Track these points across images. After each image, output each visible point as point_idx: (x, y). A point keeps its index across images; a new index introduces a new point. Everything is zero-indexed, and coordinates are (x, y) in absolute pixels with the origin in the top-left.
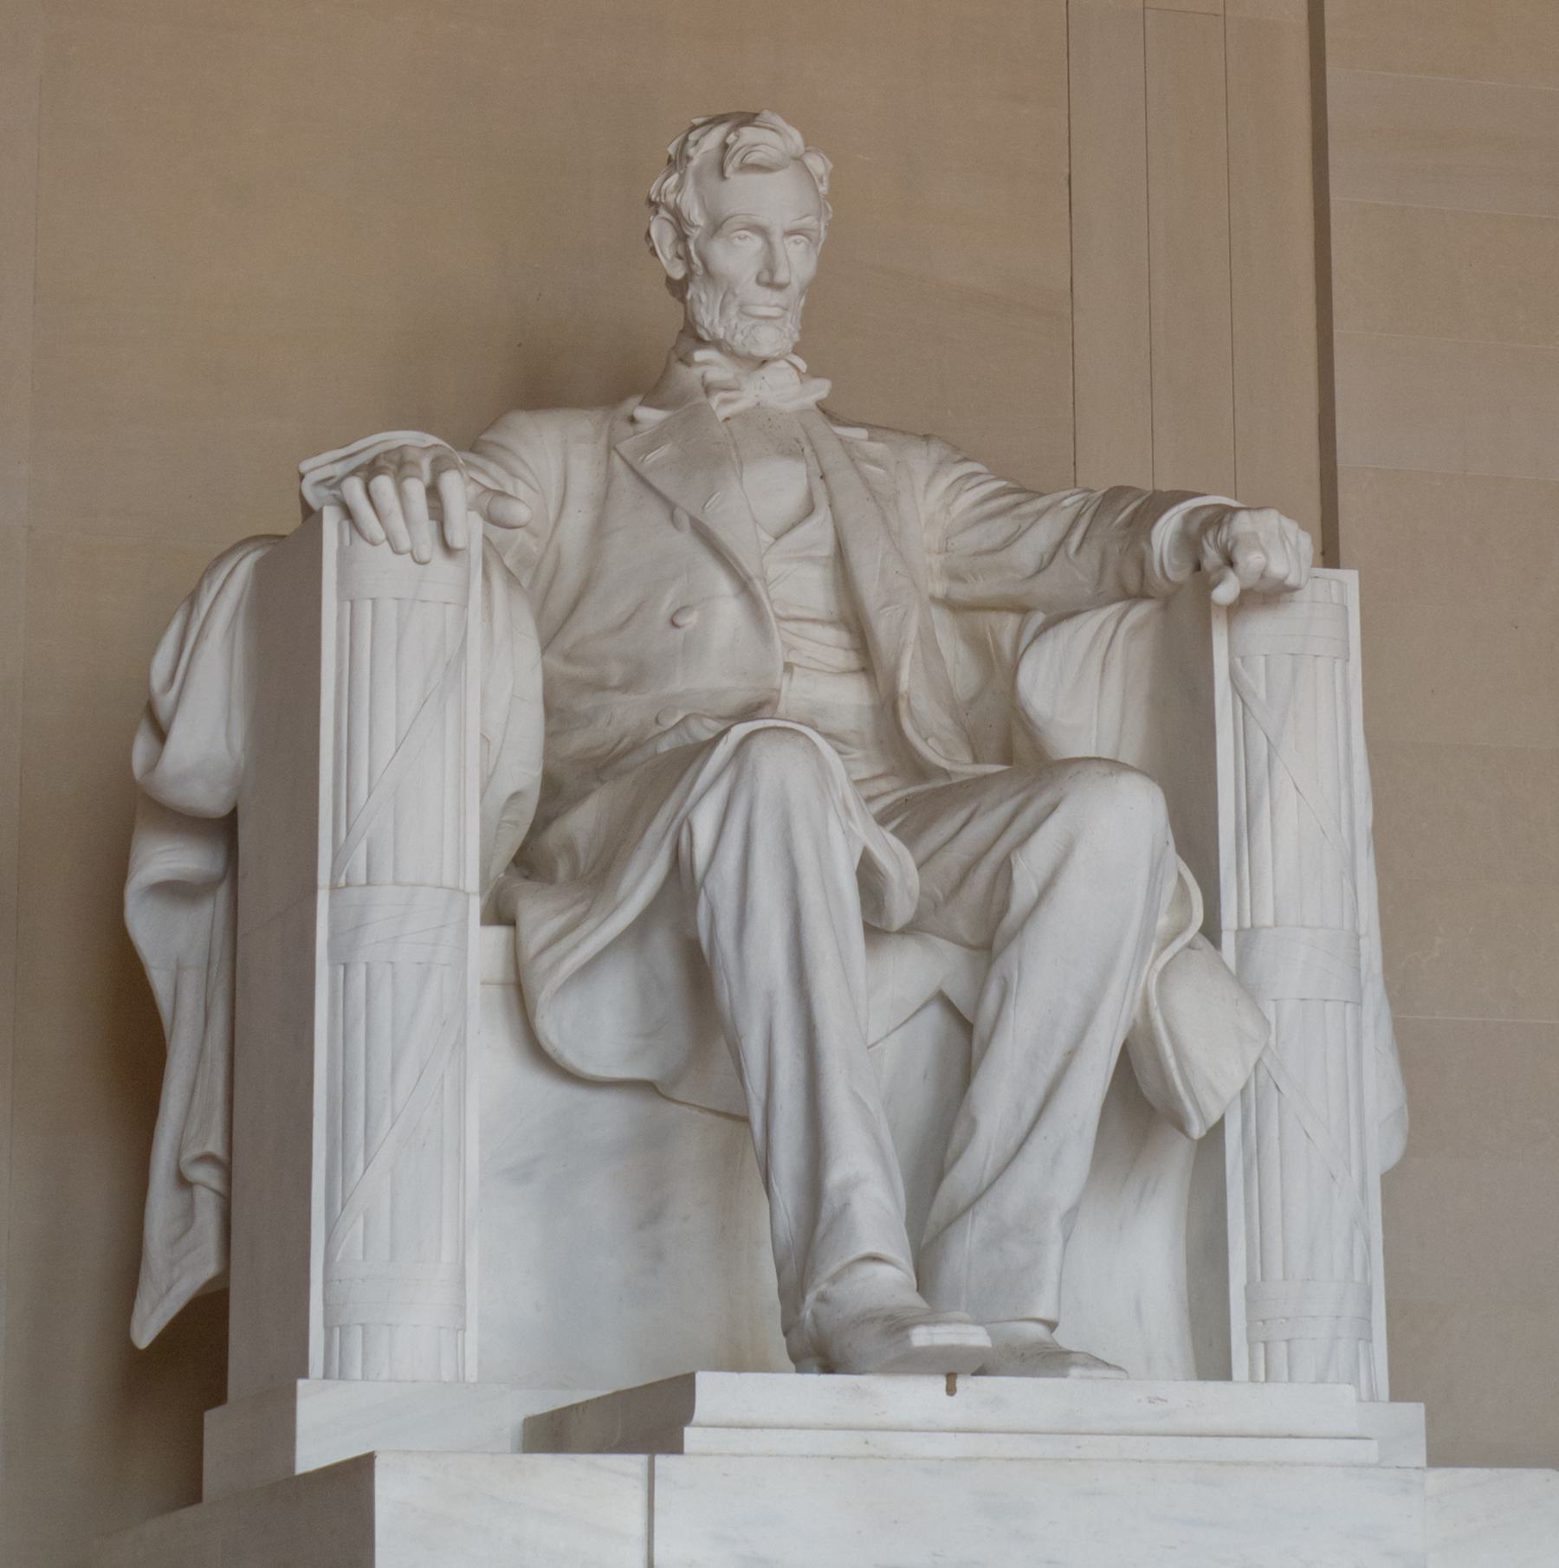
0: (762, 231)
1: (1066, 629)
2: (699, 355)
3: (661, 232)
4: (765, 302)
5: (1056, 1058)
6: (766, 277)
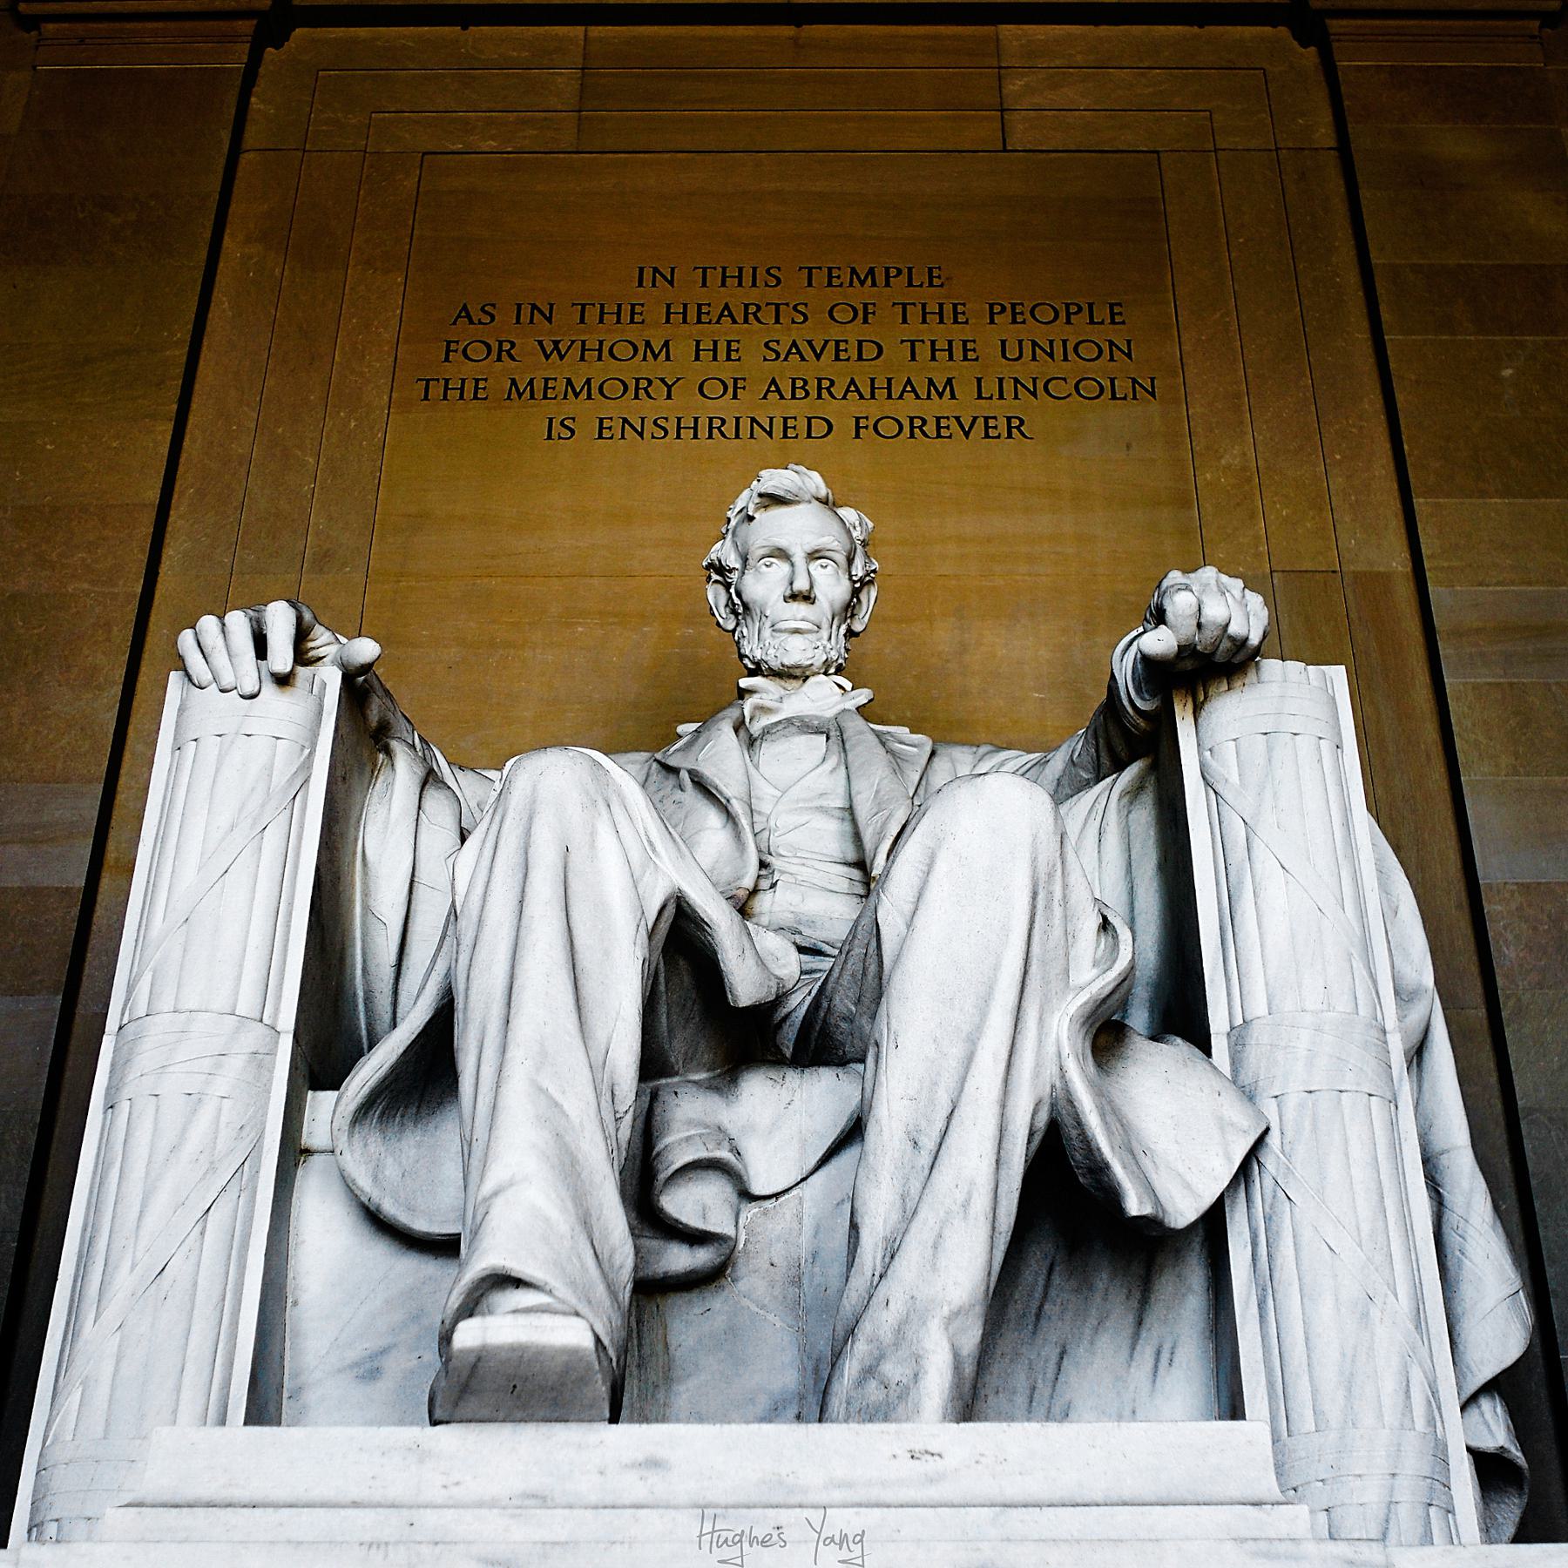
0: (782, 554)
3: (715, 595)
5: (940, 1124)
6: (788, 593)
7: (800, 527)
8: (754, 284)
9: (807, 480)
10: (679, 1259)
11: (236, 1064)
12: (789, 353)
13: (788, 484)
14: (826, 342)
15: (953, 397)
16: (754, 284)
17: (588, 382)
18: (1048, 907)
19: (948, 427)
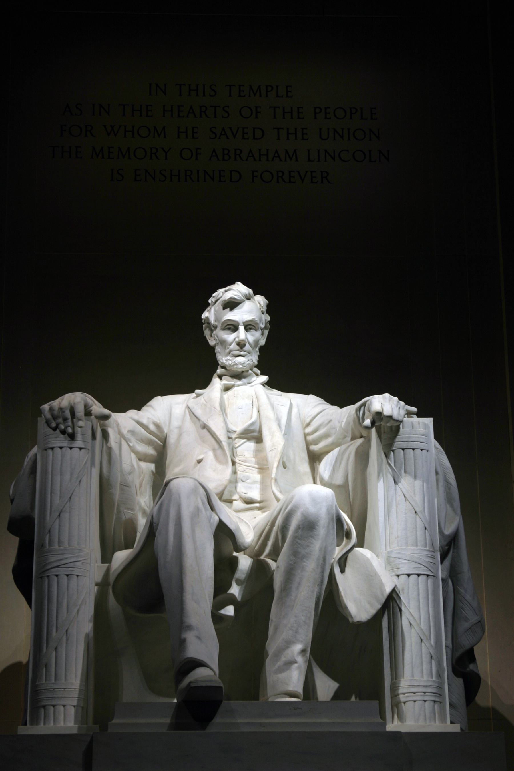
1: (336, 451)
2: (219, 371)
6: (237, 340)
8: (204, 95)
12: (221, 135)
14: (238, 128)
15: (297, 160)
16: (204, 95)
17: (129, 149)
19: (294, 177)
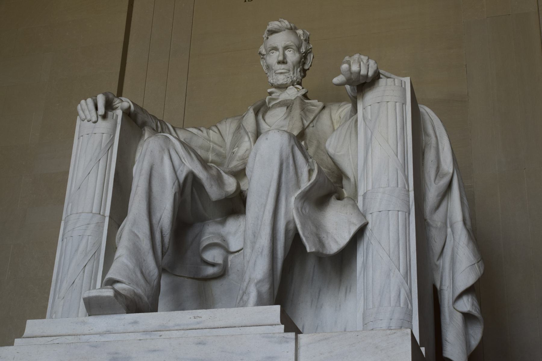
0: (276, 49)
4: (281, 68)
7: (280, 40)
9: (283, 24)
10: (210, 271)
11: (92, 226)
13: (276, 26)
18: (288, 167)
